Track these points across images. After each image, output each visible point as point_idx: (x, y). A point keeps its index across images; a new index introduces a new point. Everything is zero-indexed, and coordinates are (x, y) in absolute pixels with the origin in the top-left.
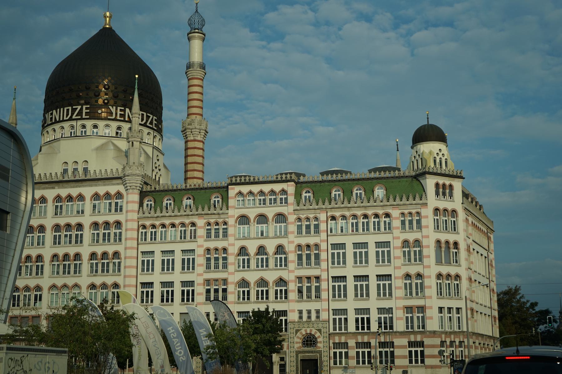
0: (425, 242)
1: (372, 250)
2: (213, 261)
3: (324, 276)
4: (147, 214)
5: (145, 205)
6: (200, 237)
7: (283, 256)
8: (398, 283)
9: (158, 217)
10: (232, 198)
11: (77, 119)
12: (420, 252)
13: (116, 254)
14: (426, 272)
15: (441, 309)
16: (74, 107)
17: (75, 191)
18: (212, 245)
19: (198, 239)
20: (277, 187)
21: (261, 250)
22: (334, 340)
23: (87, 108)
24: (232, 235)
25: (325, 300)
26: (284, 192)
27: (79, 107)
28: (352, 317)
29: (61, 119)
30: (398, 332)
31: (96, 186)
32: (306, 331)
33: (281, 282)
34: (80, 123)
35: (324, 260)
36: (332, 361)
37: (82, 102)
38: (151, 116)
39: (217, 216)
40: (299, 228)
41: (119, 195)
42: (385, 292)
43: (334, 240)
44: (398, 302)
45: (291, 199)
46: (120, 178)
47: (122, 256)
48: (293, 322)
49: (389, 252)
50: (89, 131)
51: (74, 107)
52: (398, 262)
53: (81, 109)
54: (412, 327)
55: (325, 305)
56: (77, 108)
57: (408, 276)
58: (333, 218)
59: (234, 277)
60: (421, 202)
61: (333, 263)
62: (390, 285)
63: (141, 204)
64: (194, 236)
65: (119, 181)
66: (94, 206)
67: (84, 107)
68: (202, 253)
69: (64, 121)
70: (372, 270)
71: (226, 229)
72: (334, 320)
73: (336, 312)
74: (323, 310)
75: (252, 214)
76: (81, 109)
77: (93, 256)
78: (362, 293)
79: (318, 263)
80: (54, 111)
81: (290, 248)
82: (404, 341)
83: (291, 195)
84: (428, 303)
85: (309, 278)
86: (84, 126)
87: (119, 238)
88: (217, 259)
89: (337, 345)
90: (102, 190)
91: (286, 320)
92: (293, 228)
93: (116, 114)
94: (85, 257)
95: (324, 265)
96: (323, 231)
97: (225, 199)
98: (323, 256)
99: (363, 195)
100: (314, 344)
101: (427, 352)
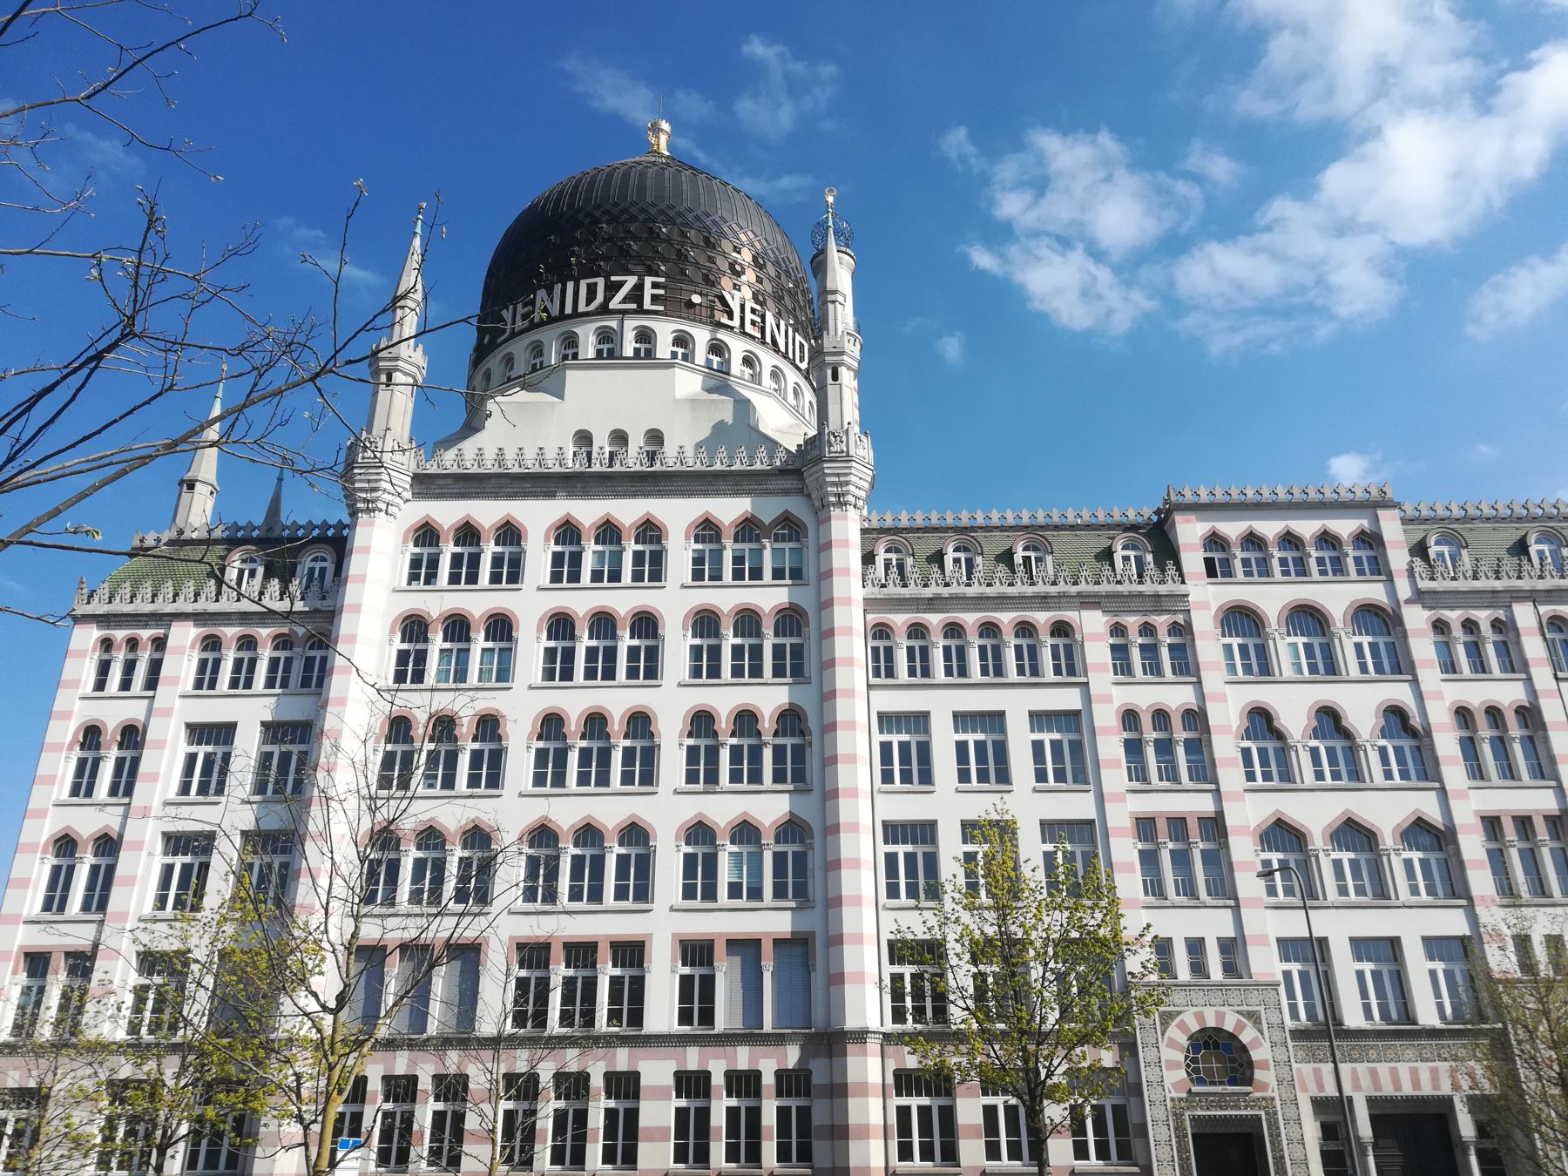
11: (624, 312)
17: (628, 511)
23: (655, 285)
27: (631, 281)
29: (568, 310)
34: (631, 325)
47: (813, 723)
50: (664, 348)
53: (639, 287)
56: (622, 284)
65: (788, 483)
67: (648, 281)
69: (576, 314)
86: (645, 336)
93: (742, 319)
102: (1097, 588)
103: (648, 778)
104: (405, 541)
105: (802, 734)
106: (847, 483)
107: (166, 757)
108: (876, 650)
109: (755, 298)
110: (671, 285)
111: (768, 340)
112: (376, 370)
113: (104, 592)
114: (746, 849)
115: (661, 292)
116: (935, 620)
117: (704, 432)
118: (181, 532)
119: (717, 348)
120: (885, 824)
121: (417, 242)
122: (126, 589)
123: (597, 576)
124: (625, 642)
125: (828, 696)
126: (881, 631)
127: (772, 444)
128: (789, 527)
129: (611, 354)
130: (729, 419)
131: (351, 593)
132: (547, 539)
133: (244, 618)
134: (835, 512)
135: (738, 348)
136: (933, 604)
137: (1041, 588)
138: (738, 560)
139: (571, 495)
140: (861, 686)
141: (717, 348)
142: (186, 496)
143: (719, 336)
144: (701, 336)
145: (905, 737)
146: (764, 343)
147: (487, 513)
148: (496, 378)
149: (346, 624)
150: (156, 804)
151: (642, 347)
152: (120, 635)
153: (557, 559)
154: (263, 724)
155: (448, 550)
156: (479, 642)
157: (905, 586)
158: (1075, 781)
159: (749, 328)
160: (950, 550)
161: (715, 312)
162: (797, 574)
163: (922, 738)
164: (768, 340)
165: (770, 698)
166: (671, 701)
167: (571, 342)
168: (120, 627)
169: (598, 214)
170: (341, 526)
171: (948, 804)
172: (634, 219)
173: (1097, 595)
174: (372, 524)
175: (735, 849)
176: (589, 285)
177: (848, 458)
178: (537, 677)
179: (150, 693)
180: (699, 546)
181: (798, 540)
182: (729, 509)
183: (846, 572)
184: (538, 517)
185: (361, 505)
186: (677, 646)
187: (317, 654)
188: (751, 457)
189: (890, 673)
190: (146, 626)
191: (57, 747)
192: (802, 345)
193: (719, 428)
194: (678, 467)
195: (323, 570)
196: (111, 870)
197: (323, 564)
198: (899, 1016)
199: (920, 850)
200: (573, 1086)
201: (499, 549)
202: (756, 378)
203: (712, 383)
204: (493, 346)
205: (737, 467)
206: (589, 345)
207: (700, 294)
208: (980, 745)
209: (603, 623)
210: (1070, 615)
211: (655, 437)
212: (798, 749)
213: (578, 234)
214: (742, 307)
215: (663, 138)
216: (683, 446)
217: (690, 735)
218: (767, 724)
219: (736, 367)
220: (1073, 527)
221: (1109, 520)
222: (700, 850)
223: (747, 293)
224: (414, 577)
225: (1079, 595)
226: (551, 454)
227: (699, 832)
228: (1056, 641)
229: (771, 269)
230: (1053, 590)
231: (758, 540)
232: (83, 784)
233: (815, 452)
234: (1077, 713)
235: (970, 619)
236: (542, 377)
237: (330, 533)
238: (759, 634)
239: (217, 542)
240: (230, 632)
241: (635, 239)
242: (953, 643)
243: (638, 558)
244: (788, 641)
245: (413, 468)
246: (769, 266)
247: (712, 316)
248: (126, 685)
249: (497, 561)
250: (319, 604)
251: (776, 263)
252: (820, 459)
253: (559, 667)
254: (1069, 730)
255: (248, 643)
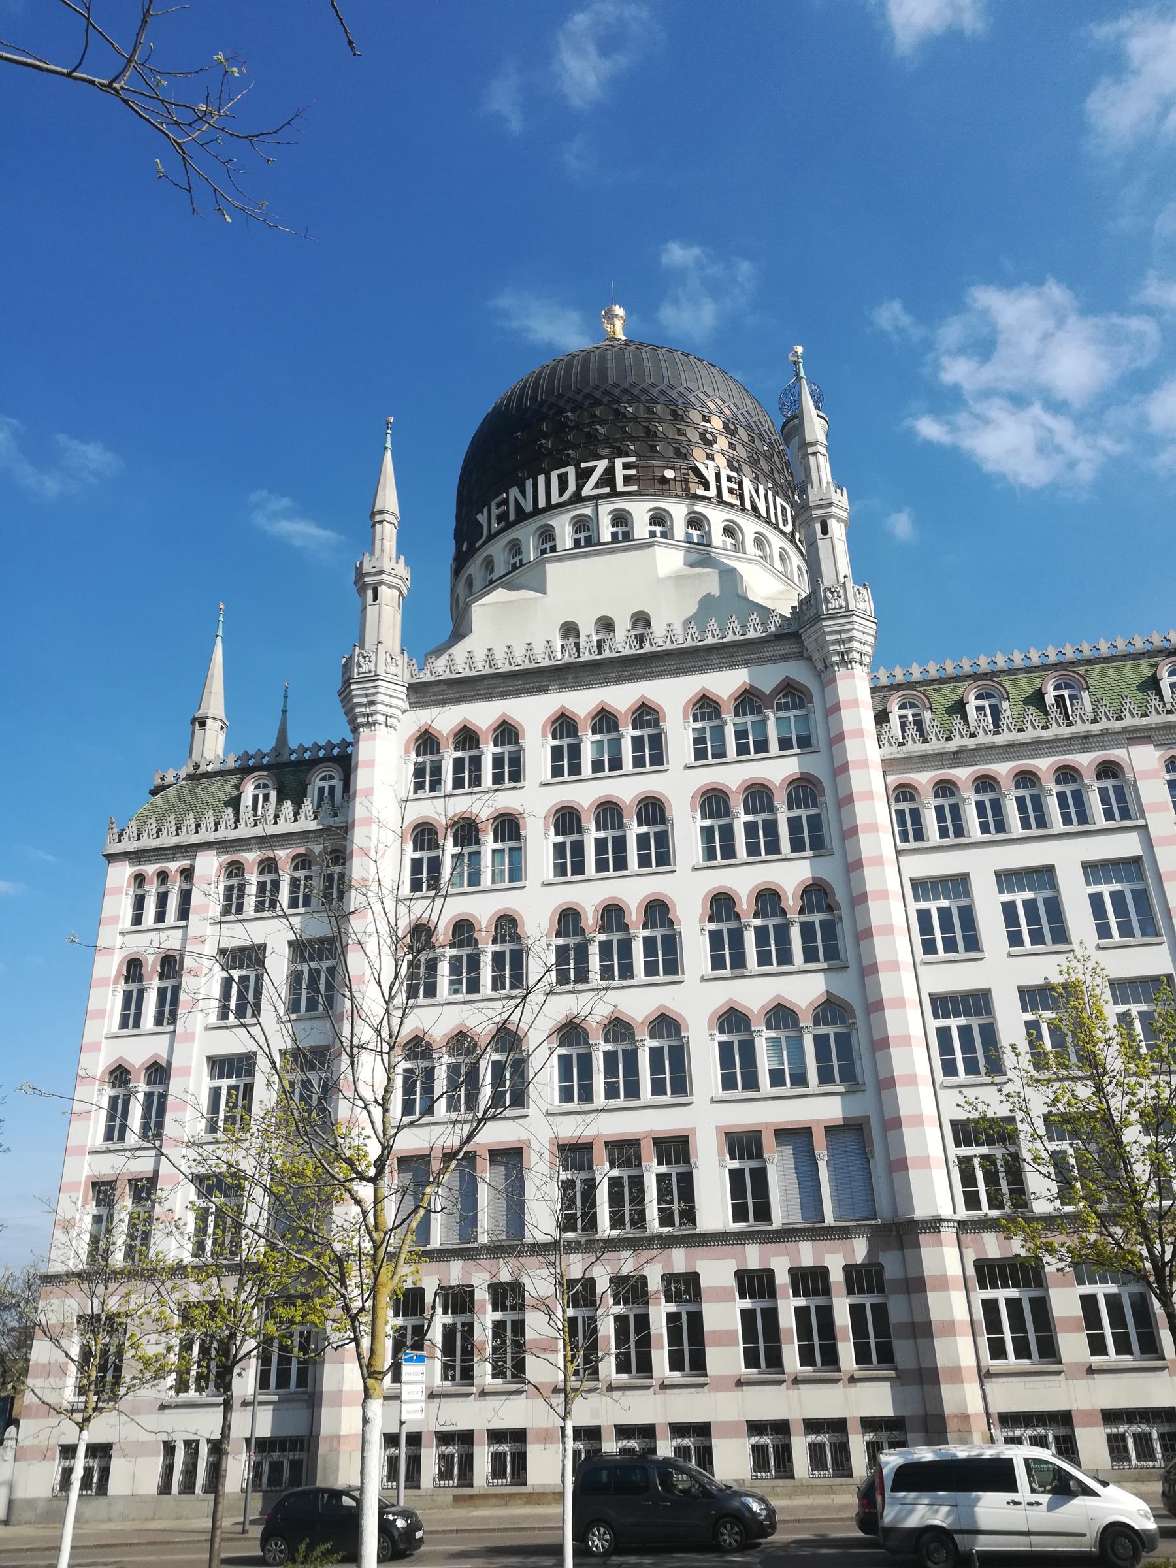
16: (583, 465)
17: (621, 697)
23: (626, 466)
27: (602, 465)
29: (542, 503)
34: (605, 510)
47: (840, 896)
50: (641, 528)
51: (583, 465)
53: (610, 470)
56: (592, 469)
65: (787, 648)
67: (619, 462)
69: (550, 507)
80: (514, 492)
86: (621, 519)
93: (719, 488)
102: (1145, 721)
103: (673, 967)
104: (407, 751)
105: (830, 908)
106: (850, 640)
107: (204, 983)
108: (900, 814)
109: (730, 465)
110: (642, 463)
111: (748, 506)
112: (365, 586)
113: (132, 830)
114: (783, 1034)
115: (634, 472)
116: (963, 774)
117: (692, 608)
118: (197, 766)
119: (696, 521)
120: (933, 998)
121: (388, 457)
122: (152, 825)
123: (597, 766)
124: (633, 830)
125: (854, 866)
126: (904, 793)
127: (765, 612)
128: (792, 694)
129: (589, 542)
130: (716, 592)
131: (360, 810)
132: (544, 735)
133: (264, 841)
134: (840, 672)
135: (717, 518)
136: (958, 758)
137: (1079, 728)
138: (741, 734)
139: (563, 687)
140: (888, 851)
141: (696, 521)
142: (198, 734)
143: (696, 509)
144: (678, 511)
145: (944, 903)
146: (744, 510)
147: (482, 714)
148: (477, 584)
149: (359, 837)
150: (199, 1028)
151: (620, 530)
152: (150, 869)
153: (557, 753)
154: (291, 944)
155: (449, 756)
156: (489, 844)
157: (925, 741)
158: (1144, 934)
159: (726, 497)
160: (972, 698)
161: (690, 484)
162: (805, 742)
163: (963, 902)
164: (748, 506)
165: (791, 874)
166: (687, 887)
167: (547, 536)
168: (149, 862)
169: (561, 403)
170: (345, 744)
171: (1002, 970)
172: (598, 402)
173: (1145, 729)
174: (373, 738)
175: (772, 1034)
176: (559, 476)
177: (848, 613)
178: (549, 874)
179: (183, 923)
180: (699, 725)
181: (802, 706)
182: (726, 683)
183: (860, 733)
184: (532, 713)
185: (361, 720)
186: (687, 830)
187: (335, 870)
188: (744, 626)
189: (919, 836)
190: (173, 859)
191: (104, 982)
192: (783, 508)
193: (707, 602)
194: (669, 646)
195: (332, 788)
196: (163, 1097)
197: (332, 783)
198: (972, 1201)
199: (975, 1022)
200: (632, 1290)
201: (498, 749)
202: (739, 547)
203: (694, 557)
204: (473, 551)
205: (730, 638)
206: (565, 535)
207: (673, 468)
208: (1030, 905)
209: (609, 812)
210: (1118, 754)
211: (642, 620)
212: (829, 923)
213: (544, 427)
214: (718, 476)
215: (618, 324)
216: (670, 625)
217: (711, 920)
218: (791, 901)
219: (718, 538)
220: (1106, 660)
221: (1149, 647)
222: (735, 1038)
223: (721, 461)
224: (419, 786)
225: (1125, 730)
226: (539, 650)
227: (732, 1019)
228: (1103, 783)
229: (743, 434)
230: (1094, 728)
231: (760, 711)
232: (130, 1017)
233: (812, 611)
234: (1137, 860)
235: (1003, 770)
236: (520, 574)
237: (335, 752)
238: (771, 808)
239: (229, 772)
240: (251, 857)
241: (602, 422)
242: (986, 797)
243: (637, 743)
244: (803, 813)
245: (407, 679)
246: (741, 431)
247: (687, 489)
248: (160, 917)
249: (498, 761)
250: (331, 821)
251: (748, 428)
252: (818, 618)
253: (569, 862)
254: (1130, 880)
255: (268, 866)
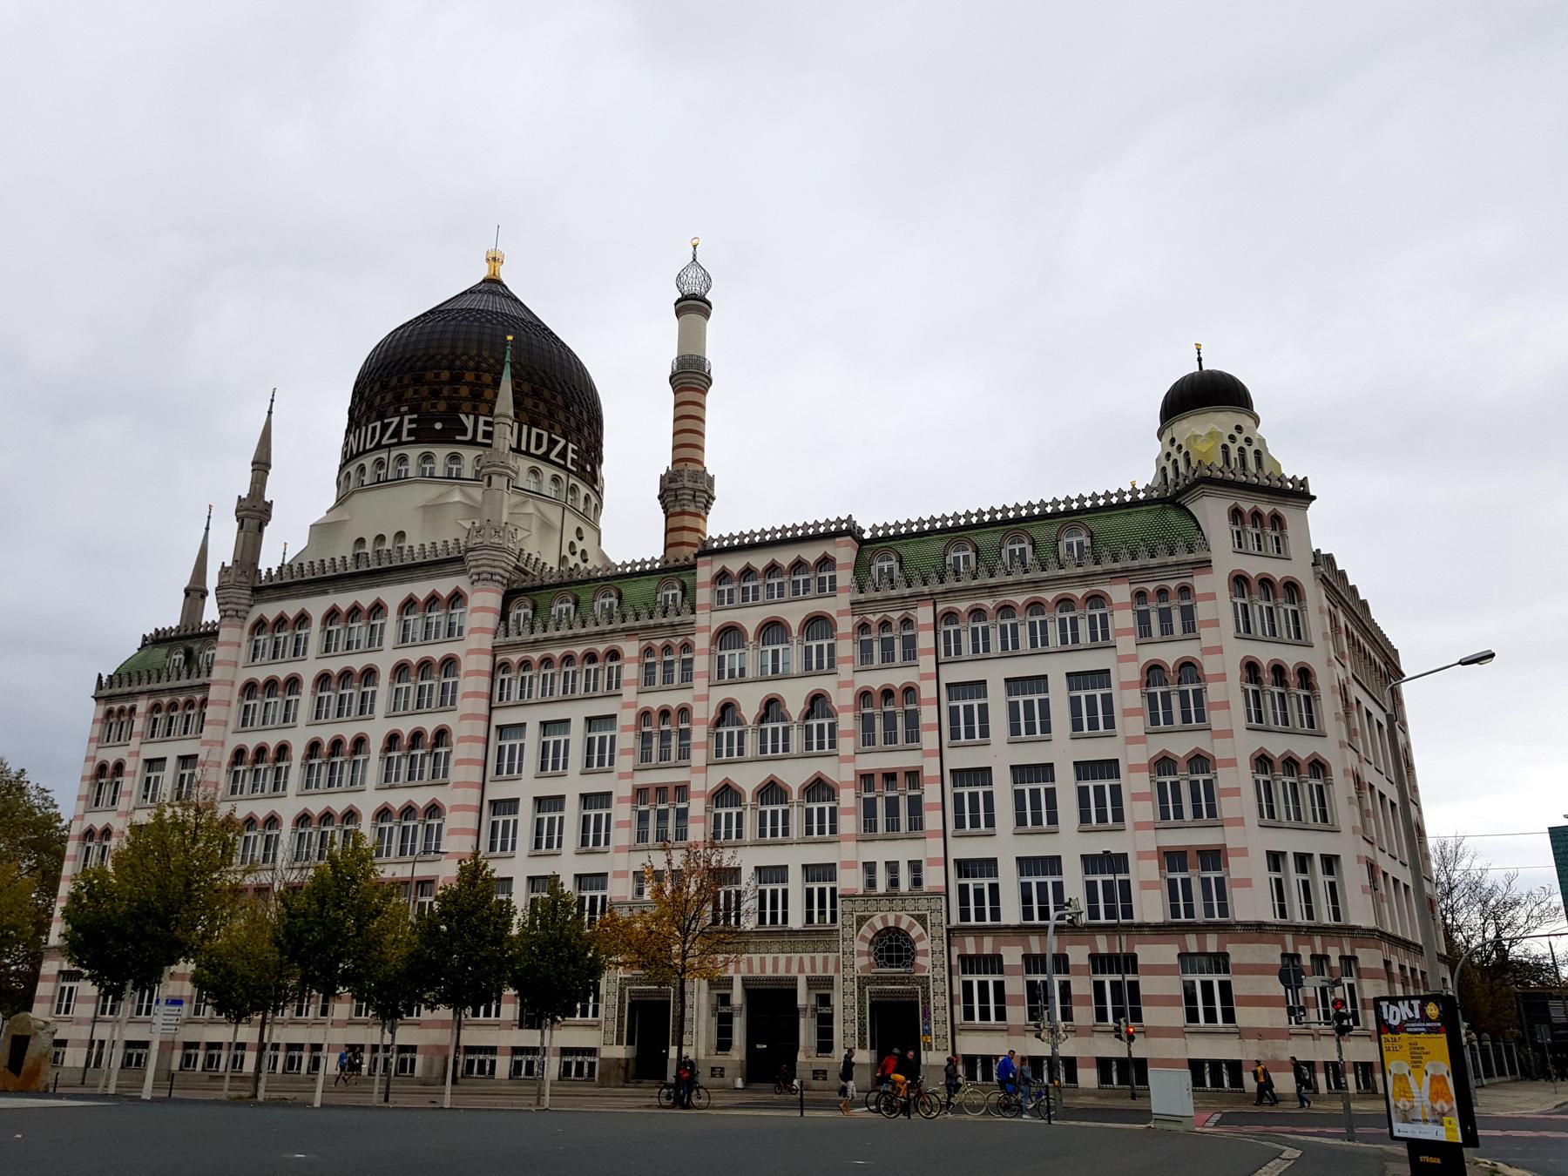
0: (1209, 666)
1: (1058, 696)
2: (656, 741)
3: (931, 768)
4: (513, 638)
5: (512, 617)
6: (629, 683)
7: (826, 722)
8: (1136, 783)
9: (536, 641)
10: (704, 585)
12: (1198, 694)
13: (441, 735)
14: (1217, 749)
15: (1275, 859)
17: (366, 598)
18: (655, 702)
19: (624, 690)
20: (811, 554)
21: (772, 707)
22: (963, 946)
23: (411, 422)
24: (701, 675)
25: (933, 834)
26: (826, 562)
27: (396, 420)
28: (1009, 881)
30: (1148, 925)
31: (411, 580)
32: (884, 919)
33: (819, 788)
34: (394, 453)
35: (929, 727)
36: (959, 1010)
37: (404, 409)
38: (563, 442)
39: (668, 632)
40: (866, 648)
41: (457, 598)
42: (1102, 807)
43: (955, 673)
44: (1139, 839)
45: (844, 577)
46: (460, 560)
48: (850, 897)
49: (1108, 700)
52: (1134, 725)
53: (400, 424)
54: (1190, 912)
55: (933, 848)
57: (1164, 764)
58: (950, 616)
59: (702, 782)
60: (1192, 557)
61: (955, 735)
62: (1116, 790)
63: (504, 616)
64: (614, 684)
65: (458, 567)
66: (406, 627)
68: (633, 722)
69: (365, 451)
70: (1062, 750)
71: (691, 660)
72: (963, 890)
73: (966, 867)
74: (932, 862)
75: (750, 619)
76: (400, 424)
77: (392, 740)
78: (1036, 811)
79: (913, 735)
81: (841, 698)
82: (1167, 953)
83: (844, 566)
84: (1229, 838)
85: (890, 777)
87: (447, 699)
88: (665, 737)
89: (970, 963)
90: (421, 589)
91: (833, 890)
92: (846, 648)
94: (376, 744)
95: (929, 739)
96: (926, 652)
97: (688, 592)
98: (928, 715)
99: (1029, 555)
100: (908, 957)
101: (1240, 985)
184: (317, 606)
211: (401, 535)
